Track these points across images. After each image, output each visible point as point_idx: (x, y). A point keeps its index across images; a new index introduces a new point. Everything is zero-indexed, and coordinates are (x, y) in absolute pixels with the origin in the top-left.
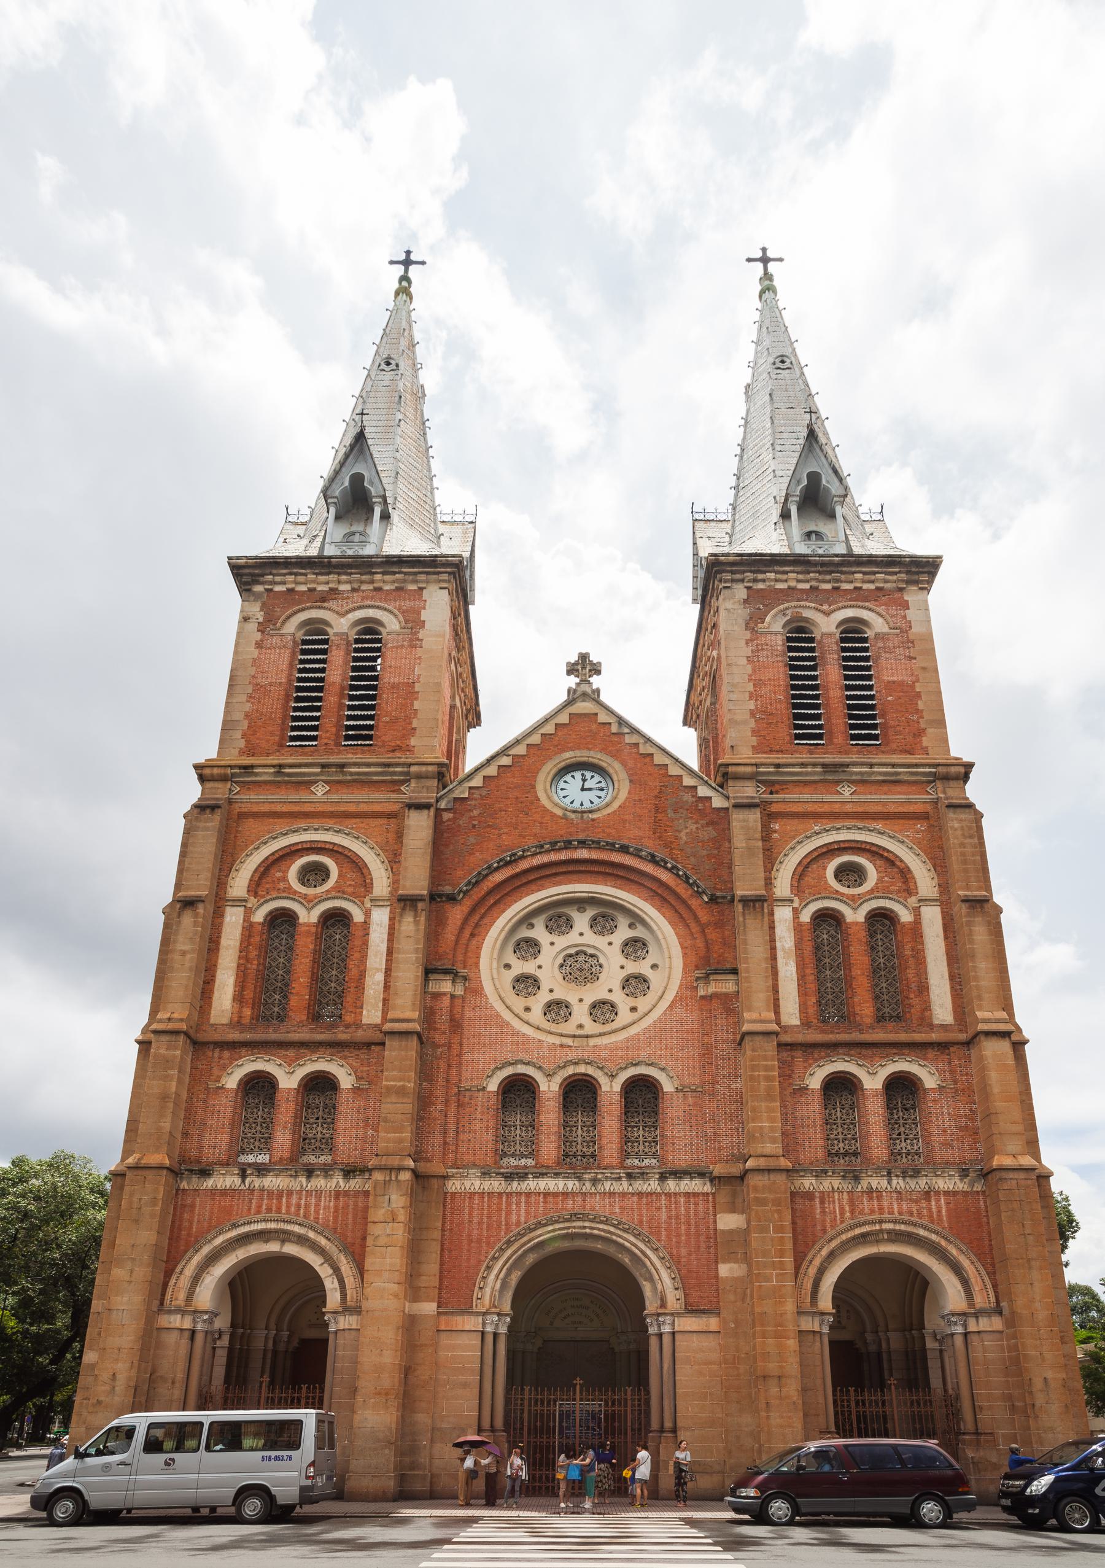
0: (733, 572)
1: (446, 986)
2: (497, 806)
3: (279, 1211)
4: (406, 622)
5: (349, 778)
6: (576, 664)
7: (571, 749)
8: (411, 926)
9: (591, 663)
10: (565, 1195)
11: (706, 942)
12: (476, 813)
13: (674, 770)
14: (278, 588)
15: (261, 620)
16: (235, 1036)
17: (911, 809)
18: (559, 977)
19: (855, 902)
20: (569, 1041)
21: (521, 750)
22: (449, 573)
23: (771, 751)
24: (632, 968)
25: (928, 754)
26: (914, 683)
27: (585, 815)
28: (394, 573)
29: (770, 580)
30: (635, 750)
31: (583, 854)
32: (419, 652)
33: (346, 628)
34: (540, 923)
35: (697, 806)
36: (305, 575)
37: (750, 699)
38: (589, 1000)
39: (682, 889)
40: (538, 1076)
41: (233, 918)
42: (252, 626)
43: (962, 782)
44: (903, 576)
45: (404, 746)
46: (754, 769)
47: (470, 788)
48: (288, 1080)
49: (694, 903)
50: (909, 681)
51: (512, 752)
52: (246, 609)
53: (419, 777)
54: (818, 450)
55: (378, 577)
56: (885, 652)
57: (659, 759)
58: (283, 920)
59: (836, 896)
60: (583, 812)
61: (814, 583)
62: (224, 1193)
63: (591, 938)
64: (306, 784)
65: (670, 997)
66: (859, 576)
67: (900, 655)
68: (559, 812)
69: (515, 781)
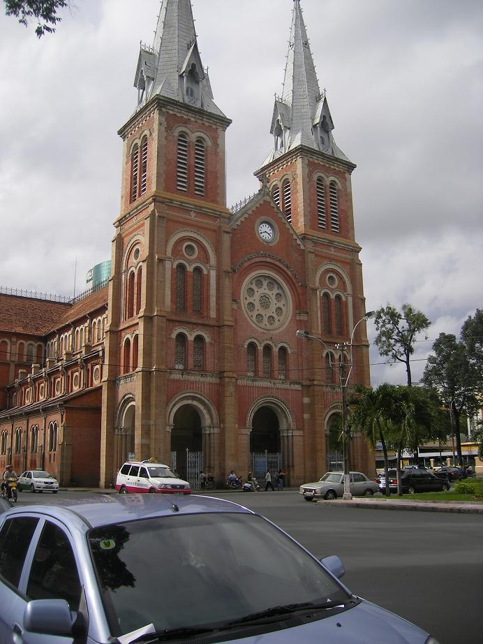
1: (235, 306)
3: (193, 389)
7: (264, 215)
8: (227, 283)
10: (267, 388)
11: (299, 300)
12: (238, 236)
13: (291, 232)
14: (171, 112)
16: (174, 318)
18: (259, 305)
19: (332, 290)
20: (265, 331)
21: (250, 212)
24: (278, 305)
31: (268, 260)
34: (254, 282)
38: (268, 316)
39: (293, 279)
40: (257, 343)
41: (168, 264)
42: (163, 129)
48: (191, 338)
49: (297, 285)
50: (346, 210)
53: (224, 217)
55: (204, 119)
58: (181, 267)
59: (329, 289)
62: (178, 381)
63: (267, 291)
64: (188, 211)
65: (290, 318)
68: (261, 240)
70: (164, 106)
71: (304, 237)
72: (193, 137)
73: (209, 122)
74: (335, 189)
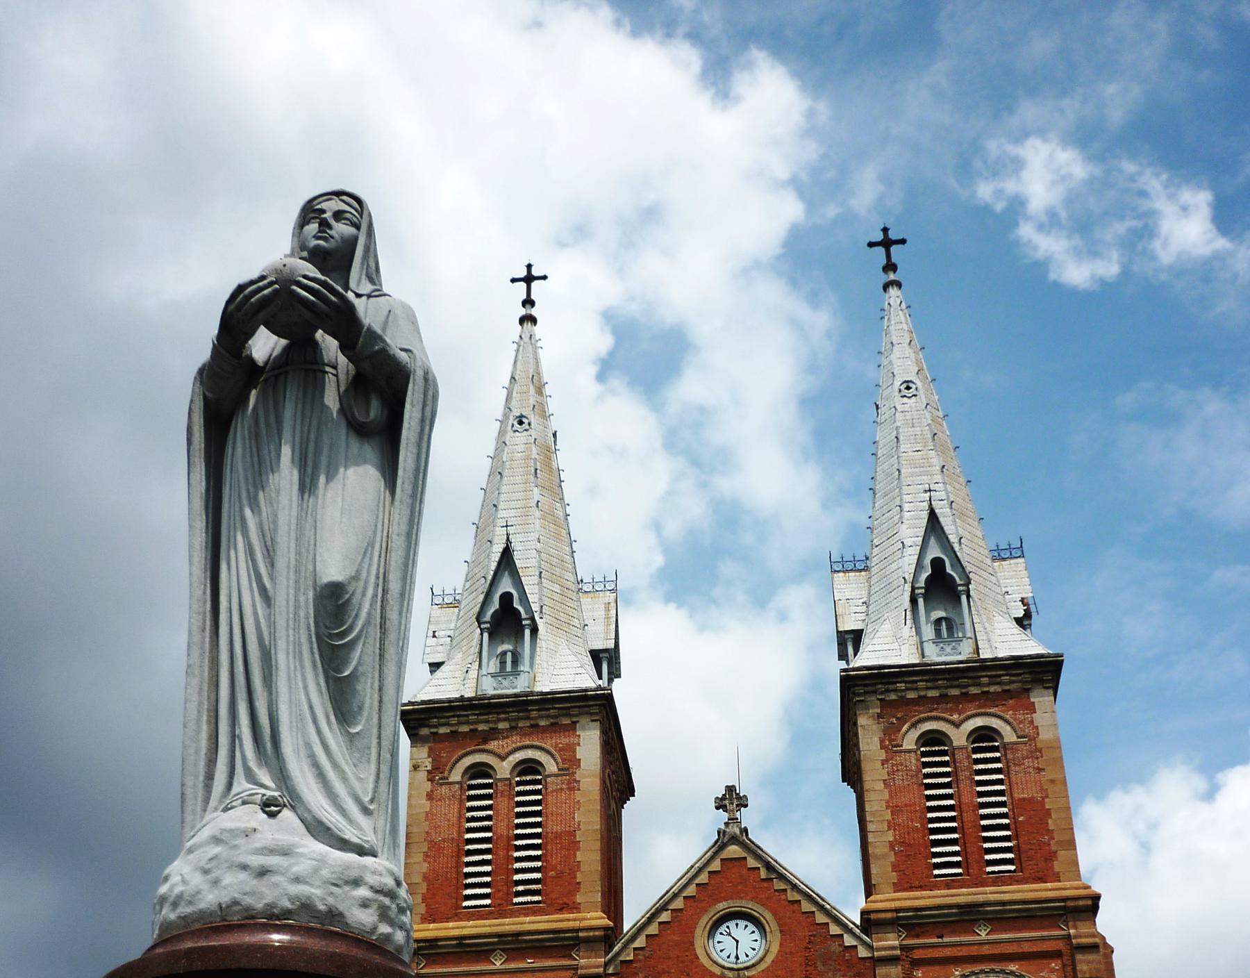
0: (865, 685)
2: (660, 967)
4: (563, 760)
5: (524, 945)
6: (724, 797)
9: (739, 797)
13: (821, 918)
14: (442, 730)
15: (429, 768)
17: (1045, 947)
21: (678, 904)
22: (599, 705)
23: (911, 887)
25: (1059, 881)
26: (1043, 798)
27: (740, 972)
28: (549, 709)
29: (903, 691)
30: (783, 897)
32: (578, 796)
33: (508, 772)
35: (844, 956)
36: (467, 716)
37: (889, 829)
42: (422, 775)
43: (1091, 914)
44: (1027, 677)
45: (571, 903)
46: (895, 915)
47: (635, 949)
50: (1039, 797)
51: (671, 907)
52: (415, 757)
53: (587, 941)
54: (940, 530)
55: (534, 714)
56: (1015, 765)
57: (806, 906)
60: (738, 970)
61: (944, 691)
66: (985, 680)
67: (1029, 767)
68: (717, 971)
69: (676, 938)
70: (423, 723)
71: (870, 922)
72: (504, 769)
73: (549, 717)
74: (995, 749)
